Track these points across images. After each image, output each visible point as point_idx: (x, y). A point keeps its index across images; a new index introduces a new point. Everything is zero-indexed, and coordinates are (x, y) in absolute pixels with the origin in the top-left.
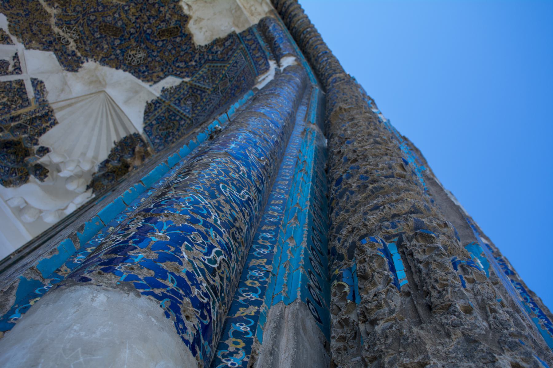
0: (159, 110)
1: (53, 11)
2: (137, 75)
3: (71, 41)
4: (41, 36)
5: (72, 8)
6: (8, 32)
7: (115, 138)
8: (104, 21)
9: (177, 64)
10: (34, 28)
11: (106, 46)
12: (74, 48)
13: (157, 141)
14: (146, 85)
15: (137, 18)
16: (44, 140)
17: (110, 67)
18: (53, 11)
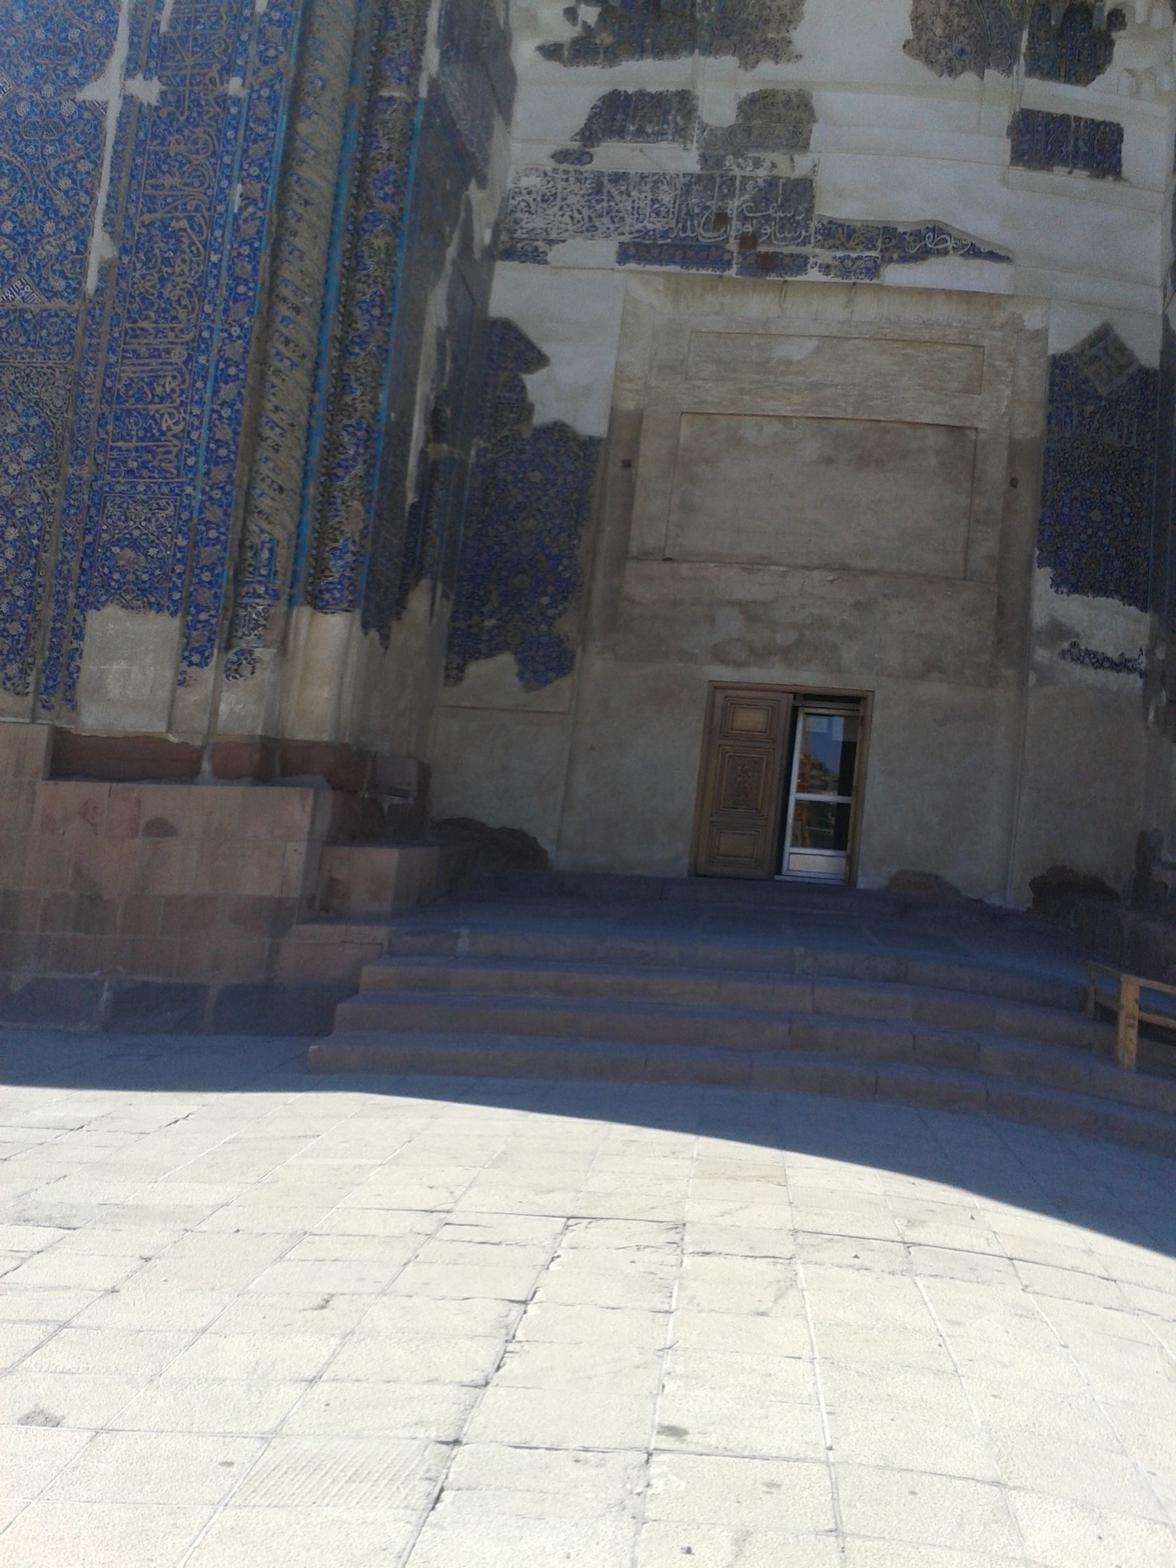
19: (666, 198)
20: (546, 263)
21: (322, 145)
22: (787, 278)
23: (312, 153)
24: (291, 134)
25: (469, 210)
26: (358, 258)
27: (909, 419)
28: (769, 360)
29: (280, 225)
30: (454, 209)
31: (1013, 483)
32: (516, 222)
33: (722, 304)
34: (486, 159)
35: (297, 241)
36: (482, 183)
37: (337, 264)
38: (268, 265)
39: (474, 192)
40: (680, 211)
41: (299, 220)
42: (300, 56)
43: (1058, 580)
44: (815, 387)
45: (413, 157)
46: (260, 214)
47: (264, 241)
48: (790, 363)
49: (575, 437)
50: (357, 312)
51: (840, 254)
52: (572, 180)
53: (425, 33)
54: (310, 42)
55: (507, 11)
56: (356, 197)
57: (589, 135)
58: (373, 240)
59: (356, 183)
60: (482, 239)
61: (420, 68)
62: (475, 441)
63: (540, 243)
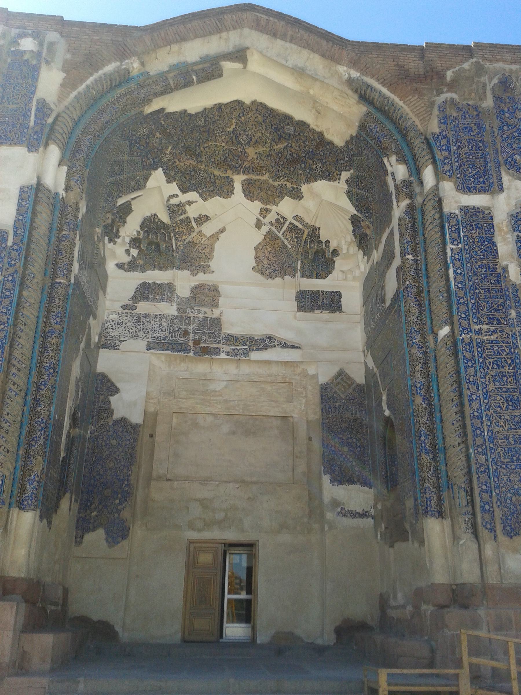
0: (354, 196)
1: (266, 177)
2: (327, 179)
3: (286, 183)
4: (275, 194)
5: (270, 167)
6: (265, 207)
7: (348, 218)
8: (287, 160)
9: (340, 162)
10: (269, 192)
11: (301, 172)
12: (291, 186)
13: (367, 215)
14: (336, 183)
15: (299, 147)
16: (323, 238)
17: (313, 182)
18: (266, 177)
19: (165, 324)
20: (119, 349)
21: (32, 301)
22: (213, 357)
23: (28, 304)
24: (20, 296)
25: (90, 328)
26: (46, 348)
27: (265, 414)
28: (207, 390)
29: (14, 333)
30: (83, 328)
31: (310, 439)
32: (107, 333)
33: (188, 367)
34: (96, 309)
35: (20, 340)
36: (95, 318)
37: (36, 351)
38: (8, 350)
39: (91, 320)
40: (170, 329)
41: (22, 332)
42: (25, 264)
43: (333, 480)
44: (226, 401)
45: (68, 307)
46: (6, 328)
47: (7, 340)
48: (216, 391)
49: (130, 424)
50: (44, 371)
51: (233, 347)
52: (129, 316)
53: (73, 257)
54: (29, 259)
55: (104, 252)
56: (45, 322)
57: (135, 299)
58: (51, 340)
59: (45, 316)
60: (95, 339)
61: (71, 271)
62: (90, 427)
63: (116, 341)
